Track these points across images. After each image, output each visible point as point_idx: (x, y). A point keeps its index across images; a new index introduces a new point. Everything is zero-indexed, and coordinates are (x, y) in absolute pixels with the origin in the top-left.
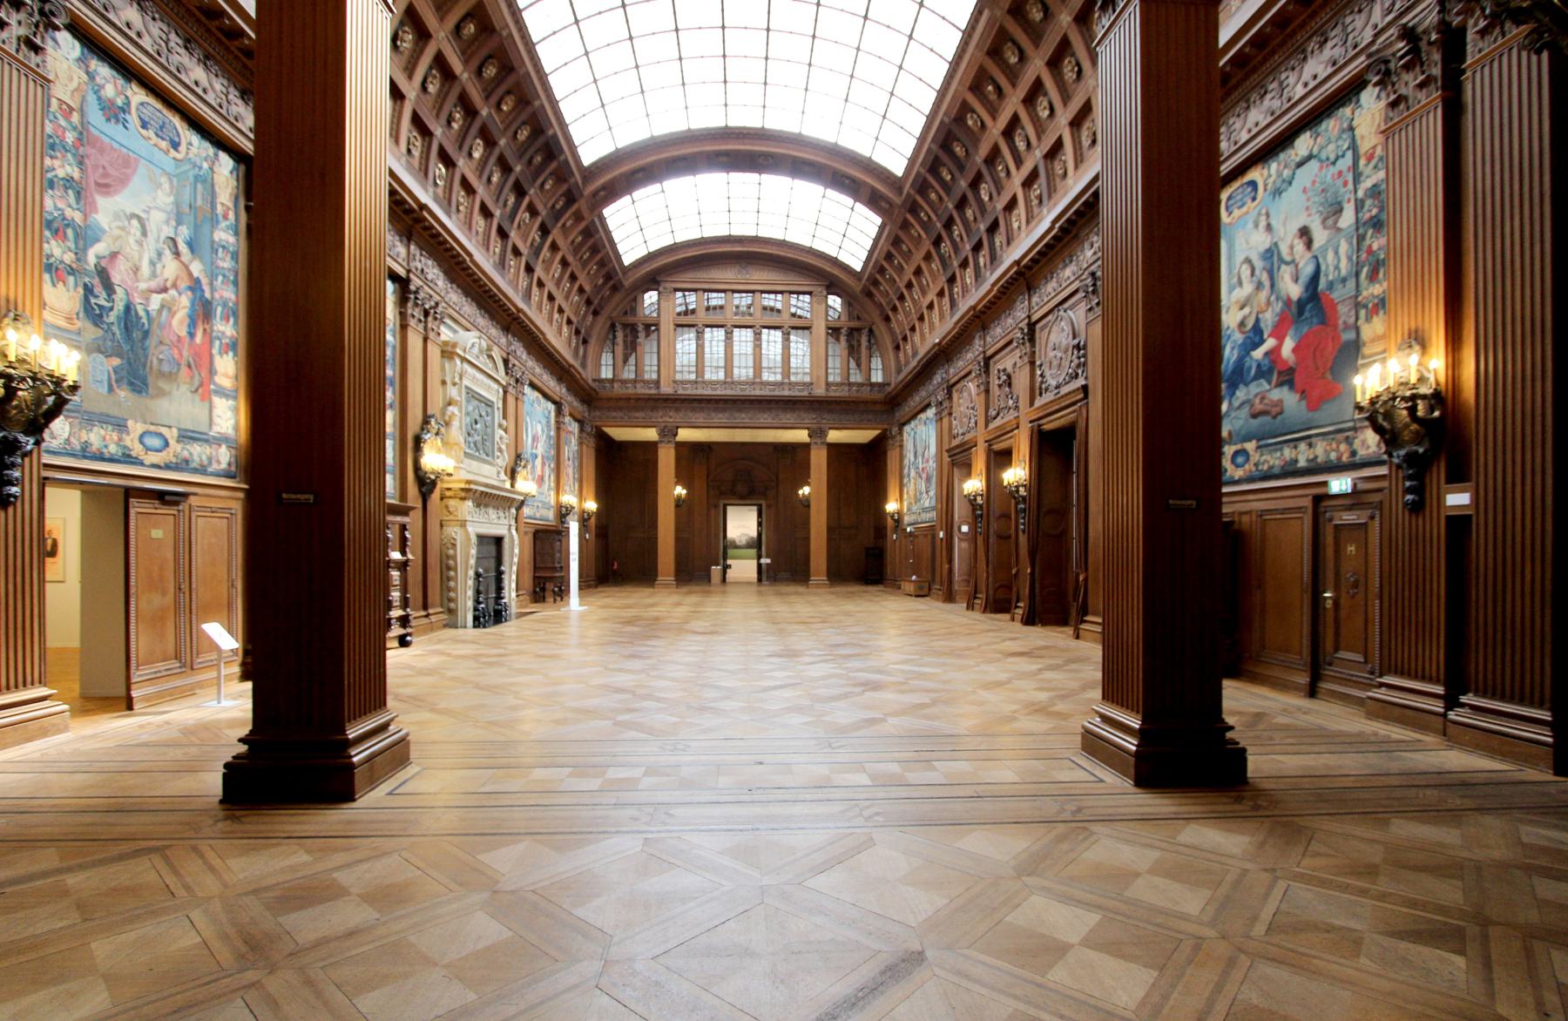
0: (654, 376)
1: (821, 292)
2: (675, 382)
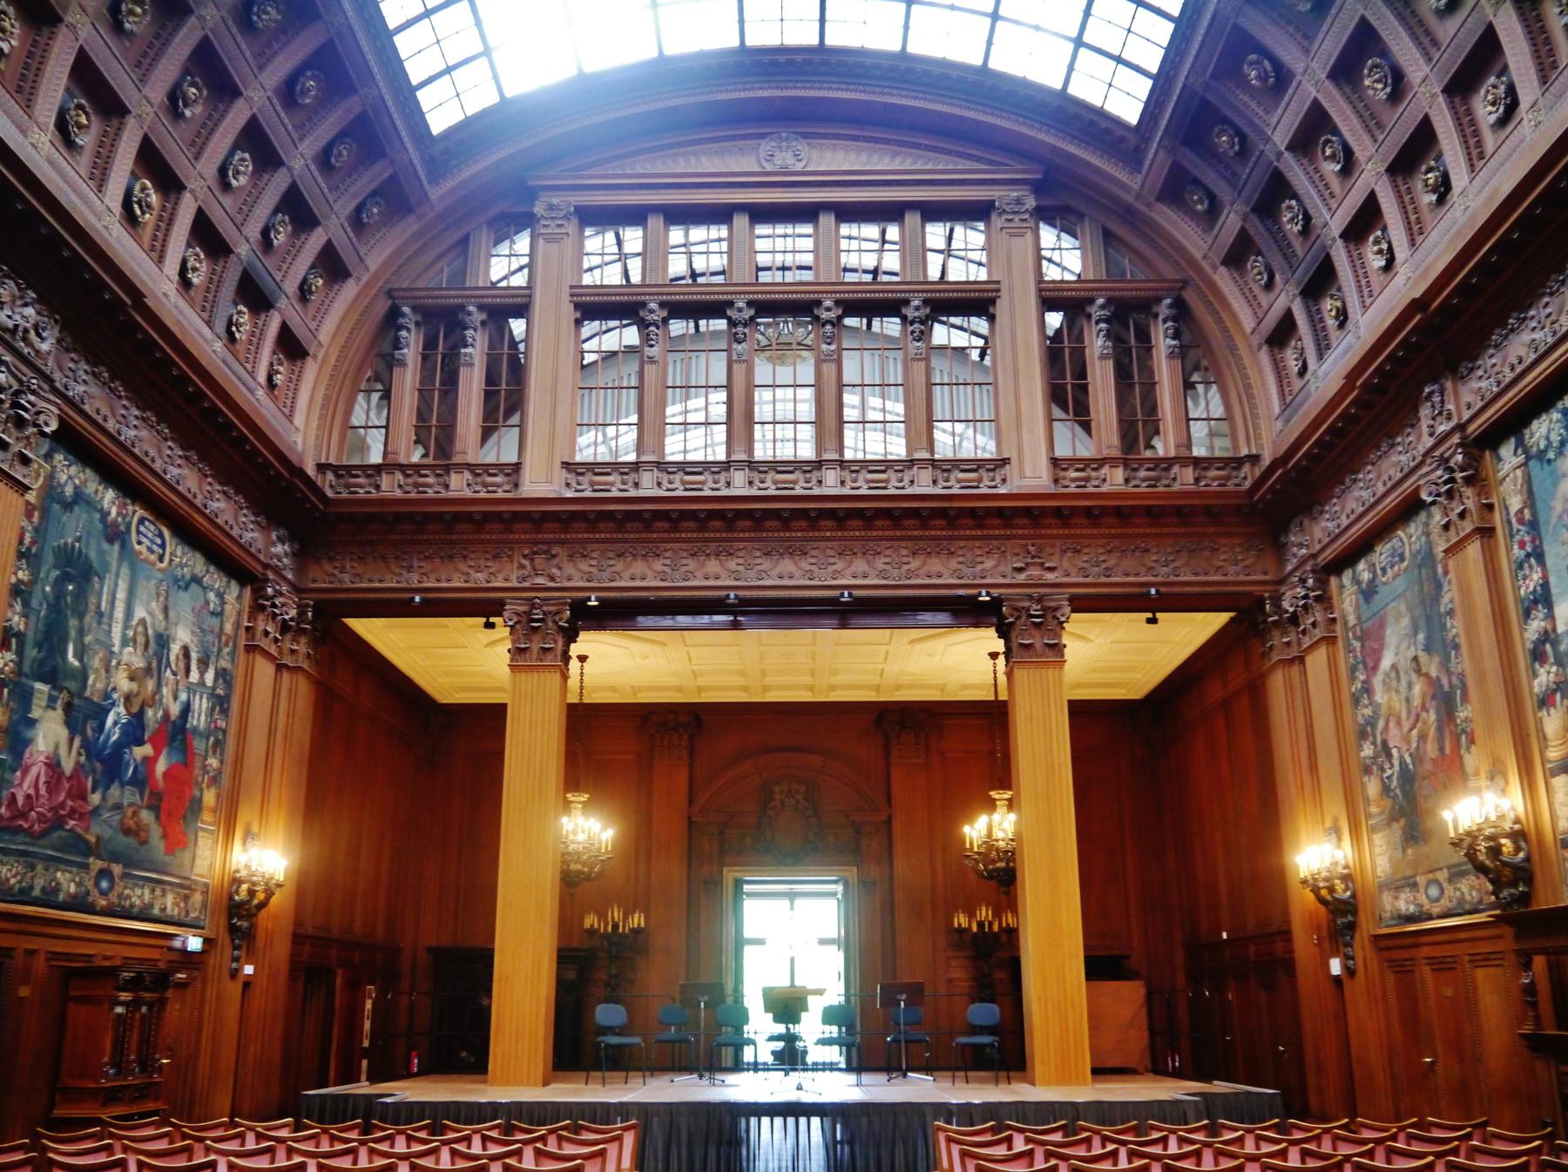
0: (514, 459)
1: (1018, 201)
2: (567, 466)
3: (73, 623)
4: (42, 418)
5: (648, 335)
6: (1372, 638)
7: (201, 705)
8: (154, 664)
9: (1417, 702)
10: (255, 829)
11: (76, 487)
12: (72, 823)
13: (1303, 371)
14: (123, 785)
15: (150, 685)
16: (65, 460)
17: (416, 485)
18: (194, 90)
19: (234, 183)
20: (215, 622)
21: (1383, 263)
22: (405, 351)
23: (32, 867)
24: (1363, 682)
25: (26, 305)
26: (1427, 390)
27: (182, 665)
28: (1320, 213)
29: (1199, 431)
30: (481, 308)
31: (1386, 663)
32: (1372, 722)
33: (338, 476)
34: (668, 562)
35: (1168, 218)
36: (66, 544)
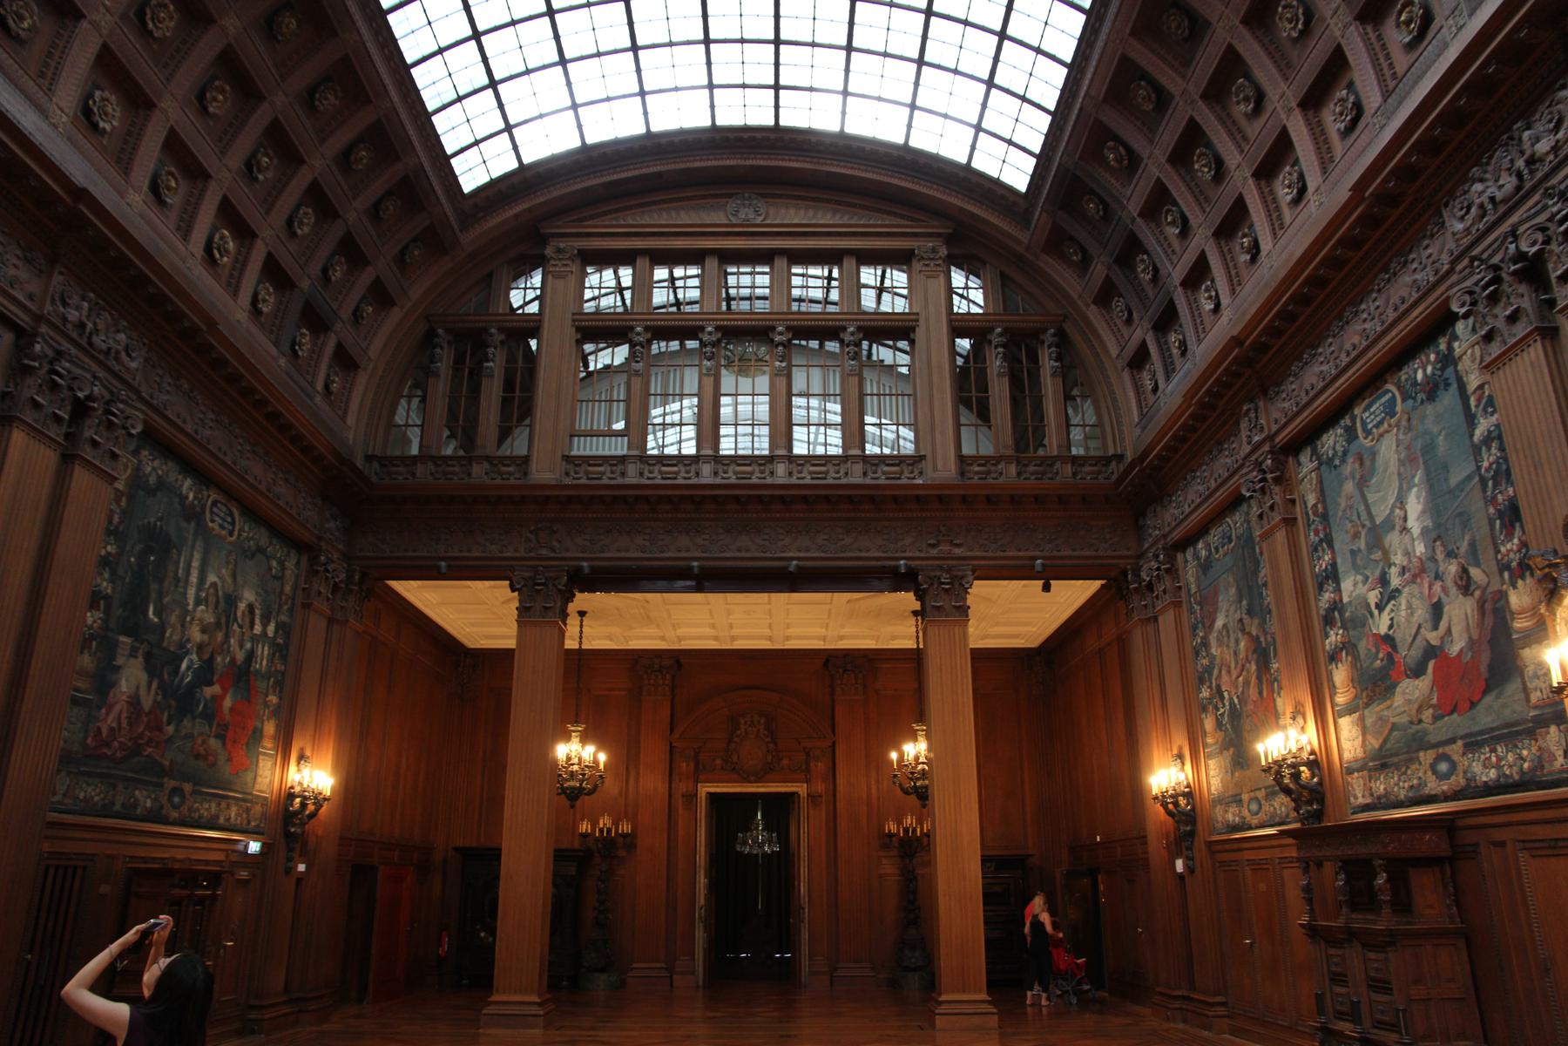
0: (525, 452)
1: (934, 250)
2: (568, 459)
3: (154, 587)
4: (130, 421)
5: (635, 353)
6: (1208, 604)
7: (264, 651)
8: (223, 620)
9: (1242, 655)
10: (308, 753)
11: (159, 477)
12: (150, 750)
13: (1155, 389)
14: (194, 718)
15: (220, 636)
16: (150, 454)
17: (444, 473)
18: (266, 159)
19: (299, 232)
20: (277, 584)
21: (1212, 306)
22: (439, 364)
23: (114, 787)
24: (1202, 638)
25: (118, 331)
26: (1245, 408)
27: (247, 620)
28: (1166, 267)
29: (1076, 434)
30: (501, 330)
31: (1219, 623)
32: (1209, 670)
33: (382, 466)
34: (647, 537)
35: (1051, 266)
36: (149, 523)
